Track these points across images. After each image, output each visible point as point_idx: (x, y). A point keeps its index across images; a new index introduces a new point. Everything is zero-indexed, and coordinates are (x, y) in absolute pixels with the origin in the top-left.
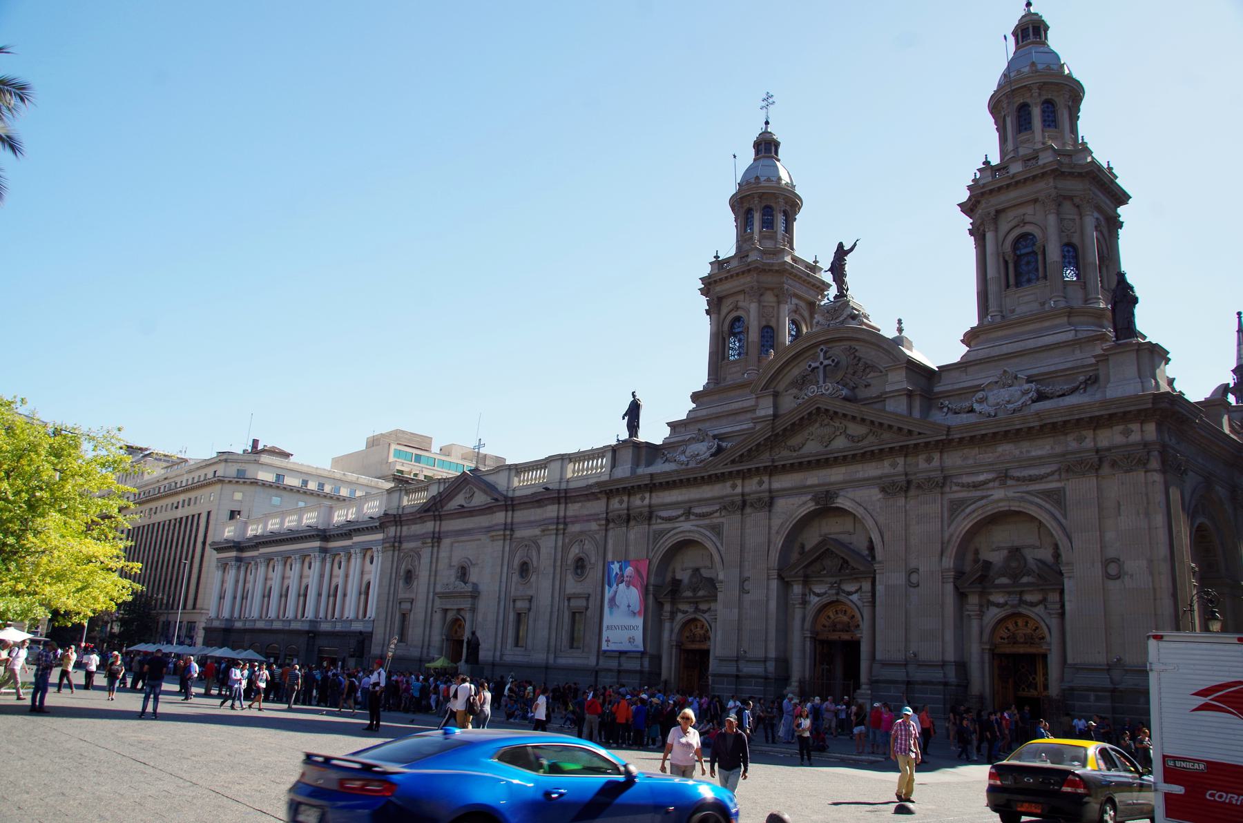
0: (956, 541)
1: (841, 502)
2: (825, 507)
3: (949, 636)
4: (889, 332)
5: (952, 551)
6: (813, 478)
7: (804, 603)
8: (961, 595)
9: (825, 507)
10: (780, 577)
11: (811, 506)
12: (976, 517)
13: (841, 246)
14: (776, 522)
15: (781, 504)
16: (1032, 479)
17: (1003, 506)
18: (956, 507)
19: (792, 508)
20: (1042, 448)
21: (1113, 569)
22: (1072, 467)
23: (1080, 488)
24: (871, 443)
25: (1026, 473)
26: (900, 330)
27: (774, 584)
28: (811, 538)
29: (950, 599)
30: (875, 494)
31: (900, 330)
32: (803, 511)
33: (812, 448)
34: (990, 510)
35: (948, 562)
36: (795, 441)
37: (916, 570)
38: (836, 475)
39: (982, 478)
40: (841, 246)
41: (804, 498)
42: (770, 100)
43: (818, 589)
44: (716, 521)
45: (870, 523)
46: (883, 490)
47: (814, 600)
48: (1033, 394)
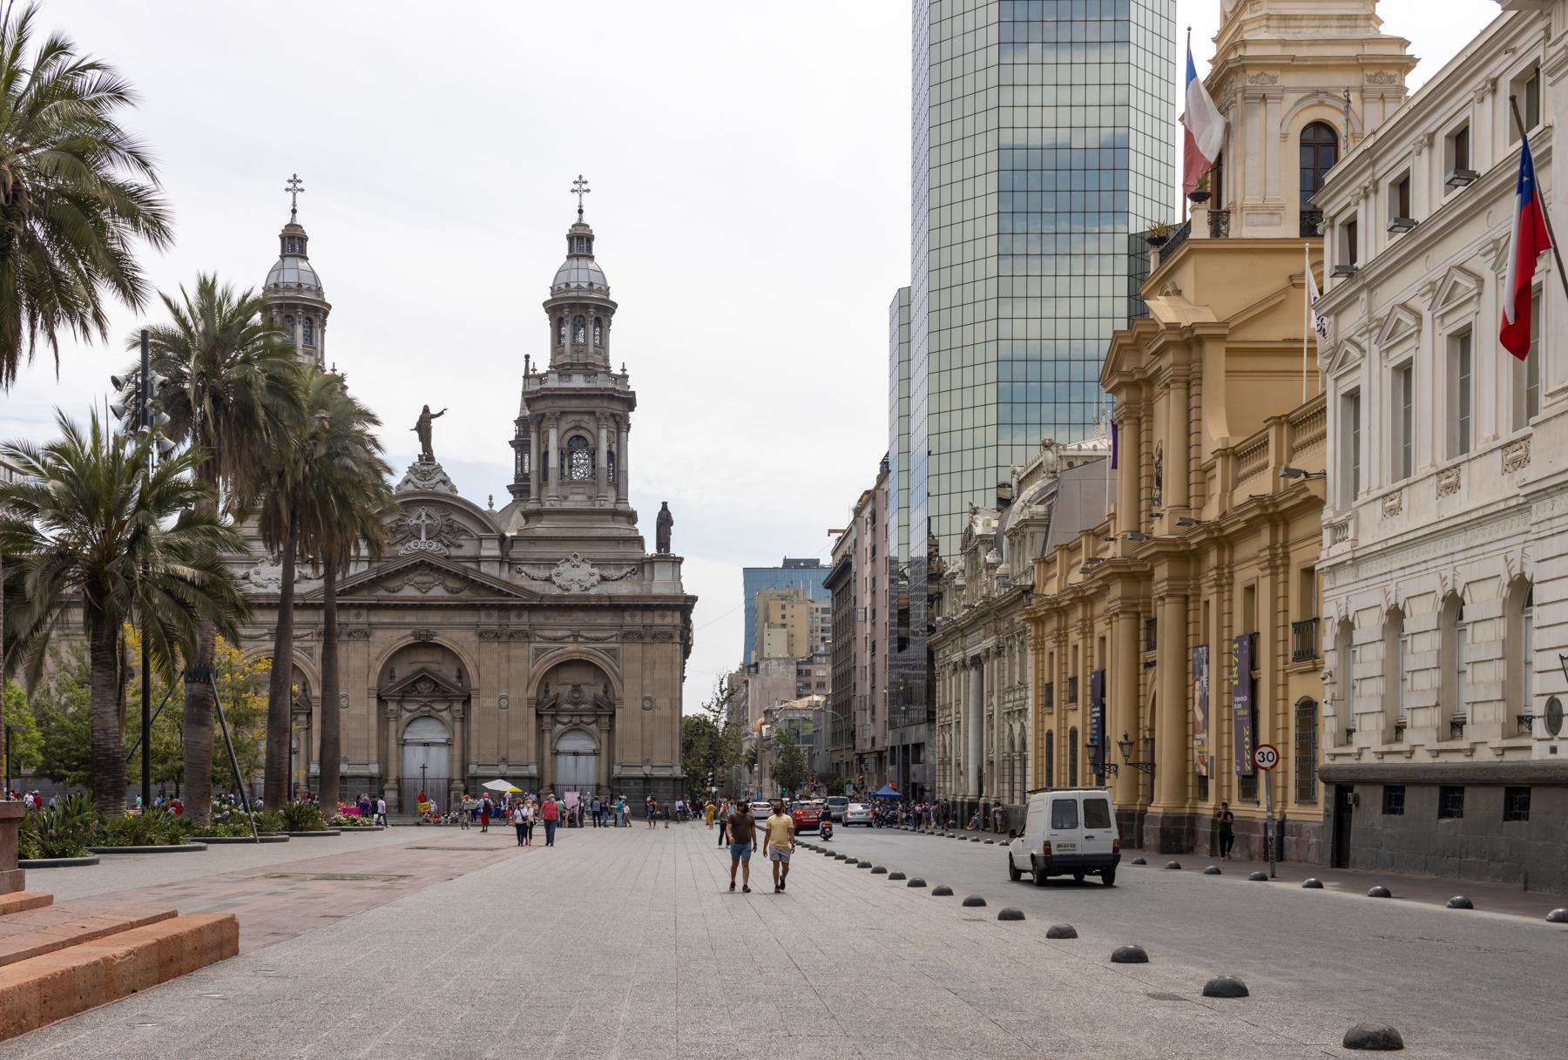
0: (539, 677)
1: (437, 640)
2: (425, 643)
3: (532, 744)
4: (485, 508)
5: (535, 685)
6: (411, 618)
7: (397, 718)
8: (539, 716)
9: (425, 643)
10: (379, 697)
11: (411, 640)
12: (555, 662)
13: (426, 409)
14: (375, 651)
15: (379, 635)
16: (597, 640)
17: (576, 656)
18: (539, 653)
20: (606, 619)
21: (647, 705)
22: (626, 637)
23: (634, 649)
24: (466, 595)
25: (593, 635)
26: (491, 505)
27: (374, 702)
29: (533, 719)
30: (471, 636)
31: (491, 505)
32: (402, 644)
33: (409, 592)
34: (566, 658)
35: (532, 693)
36: (395, 584)
37: (506, 698)
38: (434, 618)
39: (560, 634)
40: (426, 409)
41: (403, 632)
42: (299, 186)
43: (409, 707)
44: (307, 644)
45: (465, 659)
46: (481, 635)
47: (407, 715)
48: (597, 577)
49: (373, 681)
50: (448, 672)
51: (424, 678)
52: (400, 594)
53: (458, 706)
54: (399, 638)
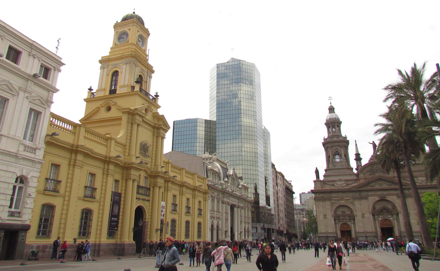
1: (387, 199)
2: (383, 199)
6: (379, 193)
9: (383, 199)
10: (372, 214)
15: (370, 198)
19: (373, 199)
28: (378, 207)
33: (377, 187)
36: (373, 184)
38: (386, 193)
41: (376, 197)
49: (370, 210)
50: (389, 206)
51: (384, 209)
52: (375, 187)
53: (395, 216)
54: (377, 198)
